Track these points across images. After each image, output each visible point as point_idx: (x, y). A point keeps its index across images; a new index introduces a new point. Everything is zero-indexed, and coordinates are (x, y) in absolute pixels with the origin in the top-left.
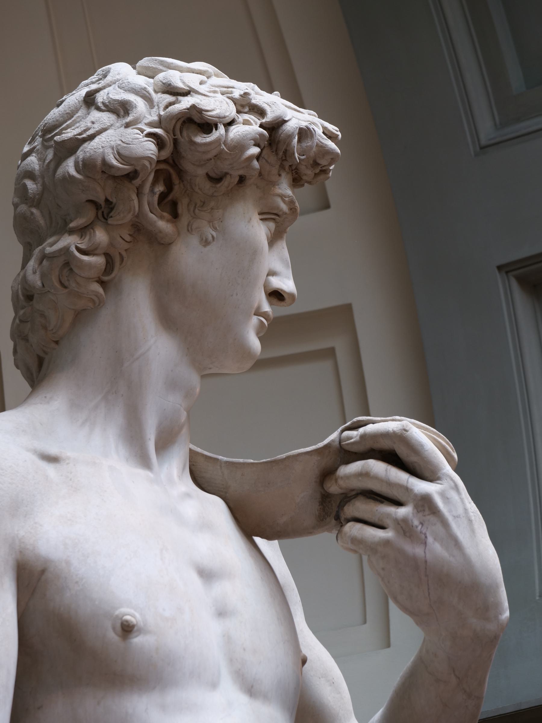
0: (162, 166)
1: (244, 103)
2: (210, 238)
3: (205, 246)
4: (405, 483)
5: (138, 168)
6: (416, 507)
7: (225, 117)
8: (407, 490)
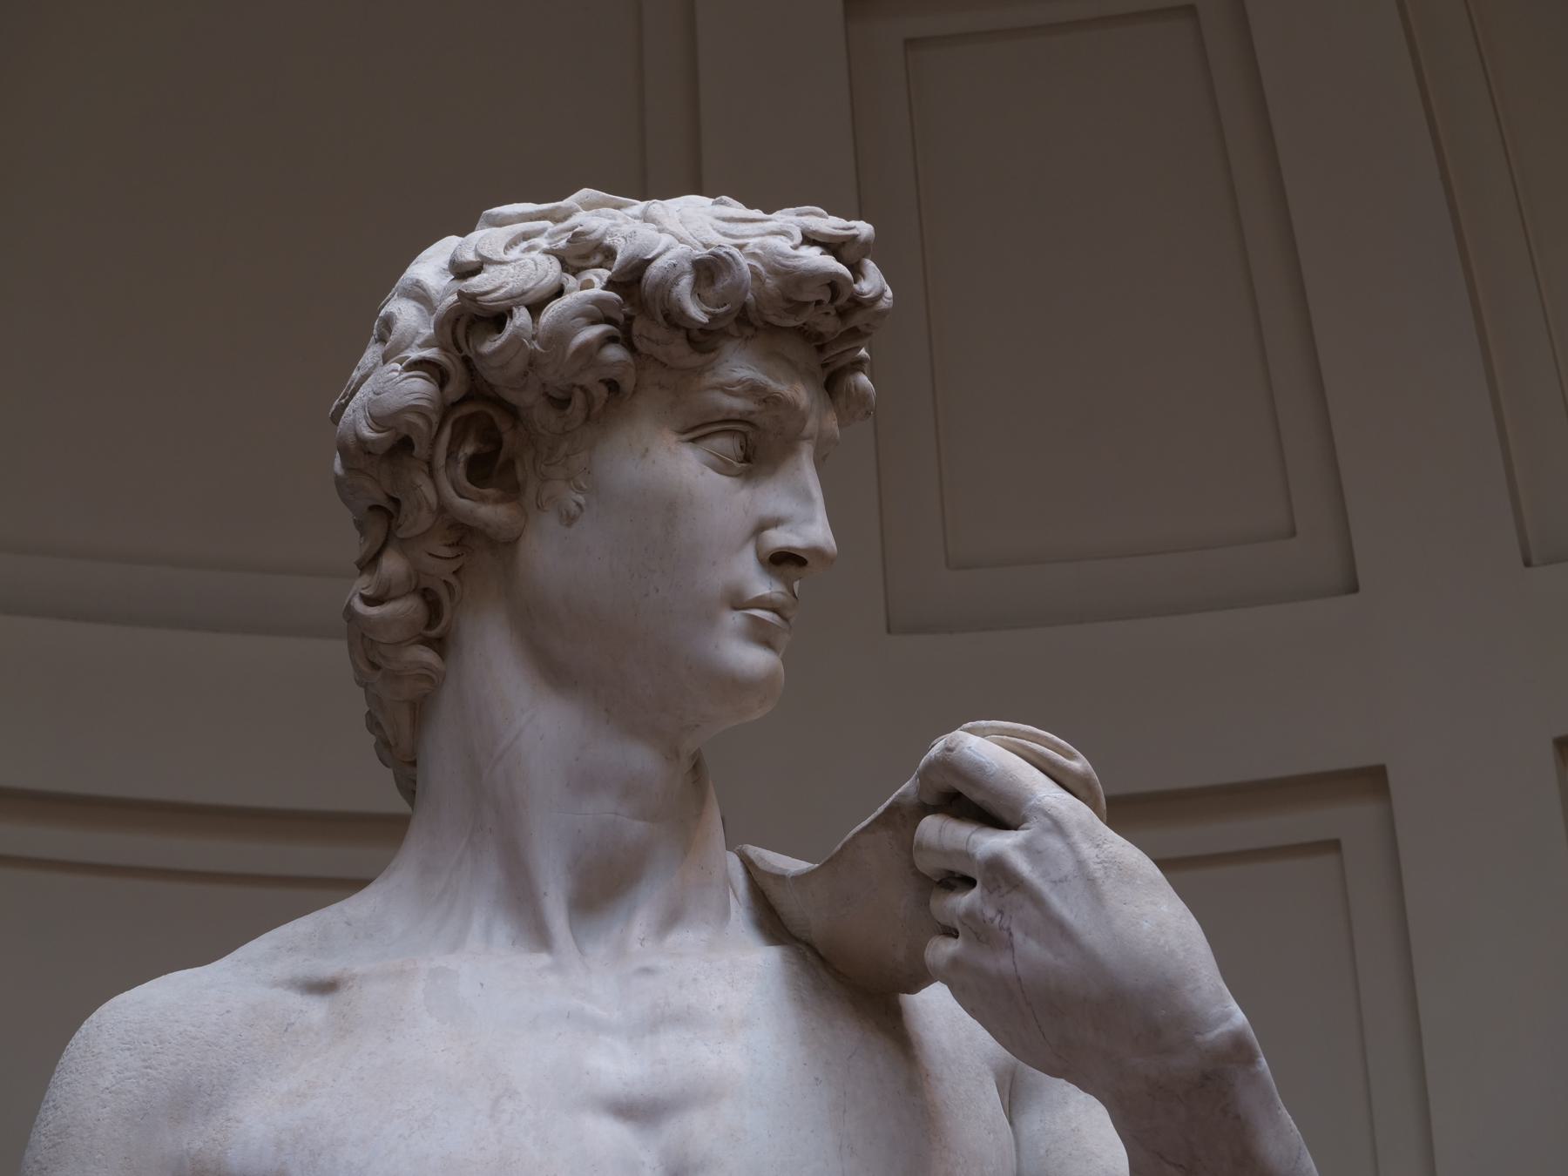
0: (466, 410)
1: (583, 251)
2: (573, 508)
3: (569, 525)
4: (963, 846)
5: (404, 431)
6: (985, 885)
7: (524, 293)
8: (967, 856)
